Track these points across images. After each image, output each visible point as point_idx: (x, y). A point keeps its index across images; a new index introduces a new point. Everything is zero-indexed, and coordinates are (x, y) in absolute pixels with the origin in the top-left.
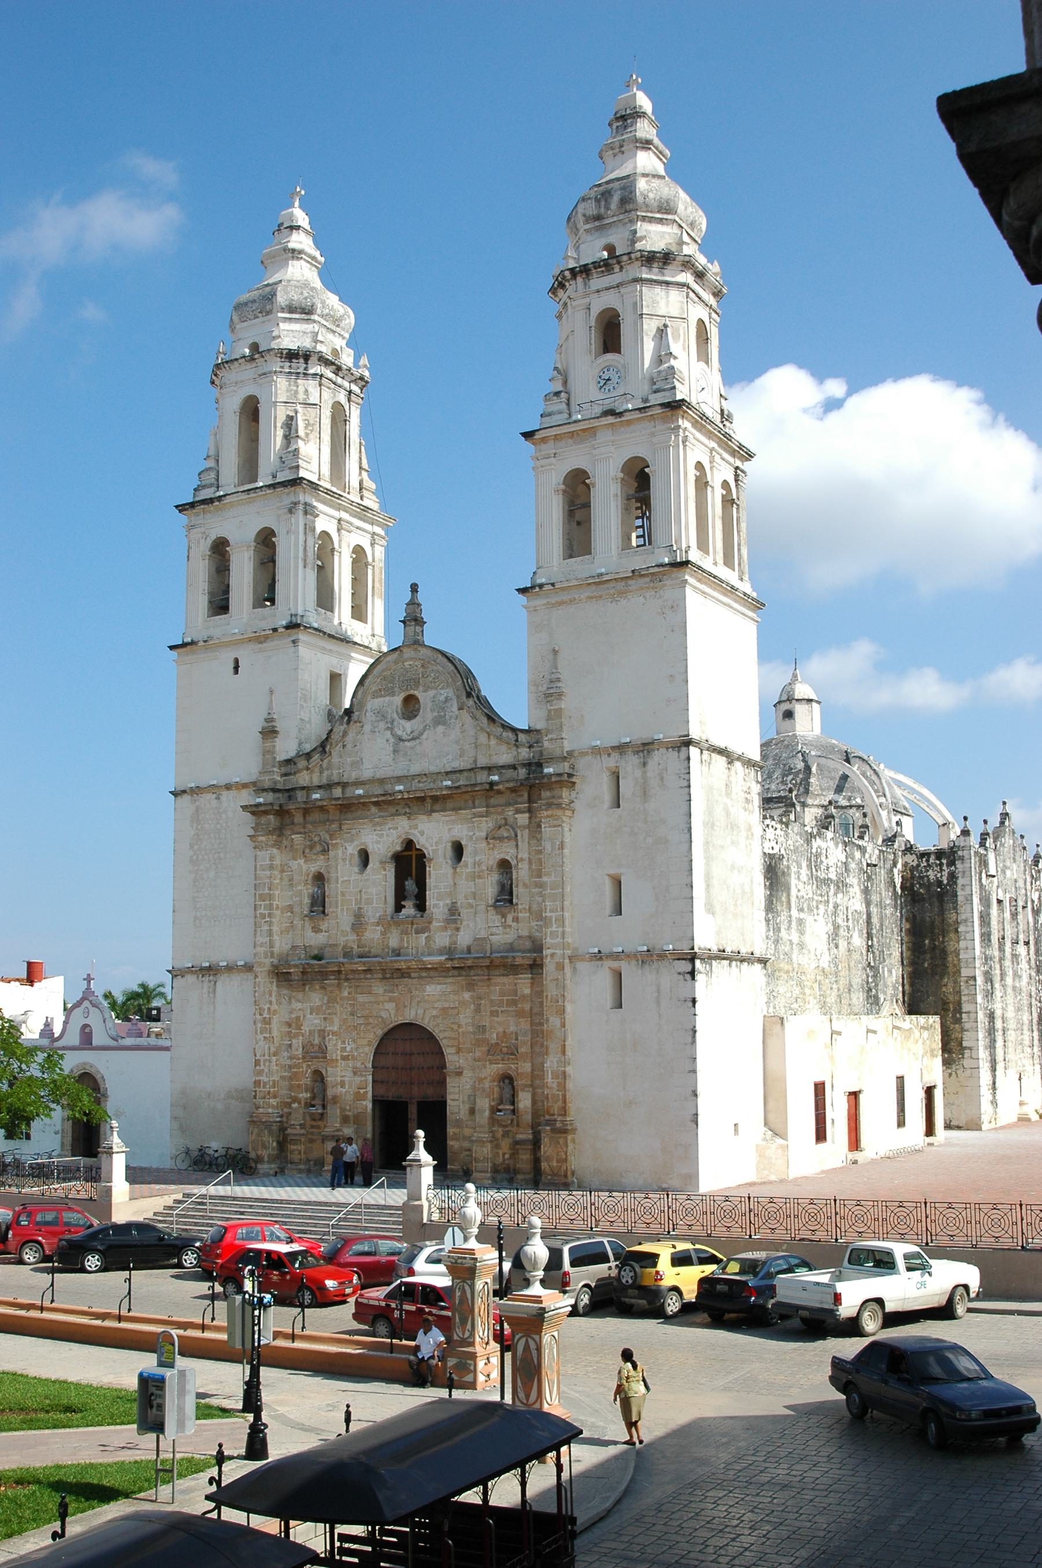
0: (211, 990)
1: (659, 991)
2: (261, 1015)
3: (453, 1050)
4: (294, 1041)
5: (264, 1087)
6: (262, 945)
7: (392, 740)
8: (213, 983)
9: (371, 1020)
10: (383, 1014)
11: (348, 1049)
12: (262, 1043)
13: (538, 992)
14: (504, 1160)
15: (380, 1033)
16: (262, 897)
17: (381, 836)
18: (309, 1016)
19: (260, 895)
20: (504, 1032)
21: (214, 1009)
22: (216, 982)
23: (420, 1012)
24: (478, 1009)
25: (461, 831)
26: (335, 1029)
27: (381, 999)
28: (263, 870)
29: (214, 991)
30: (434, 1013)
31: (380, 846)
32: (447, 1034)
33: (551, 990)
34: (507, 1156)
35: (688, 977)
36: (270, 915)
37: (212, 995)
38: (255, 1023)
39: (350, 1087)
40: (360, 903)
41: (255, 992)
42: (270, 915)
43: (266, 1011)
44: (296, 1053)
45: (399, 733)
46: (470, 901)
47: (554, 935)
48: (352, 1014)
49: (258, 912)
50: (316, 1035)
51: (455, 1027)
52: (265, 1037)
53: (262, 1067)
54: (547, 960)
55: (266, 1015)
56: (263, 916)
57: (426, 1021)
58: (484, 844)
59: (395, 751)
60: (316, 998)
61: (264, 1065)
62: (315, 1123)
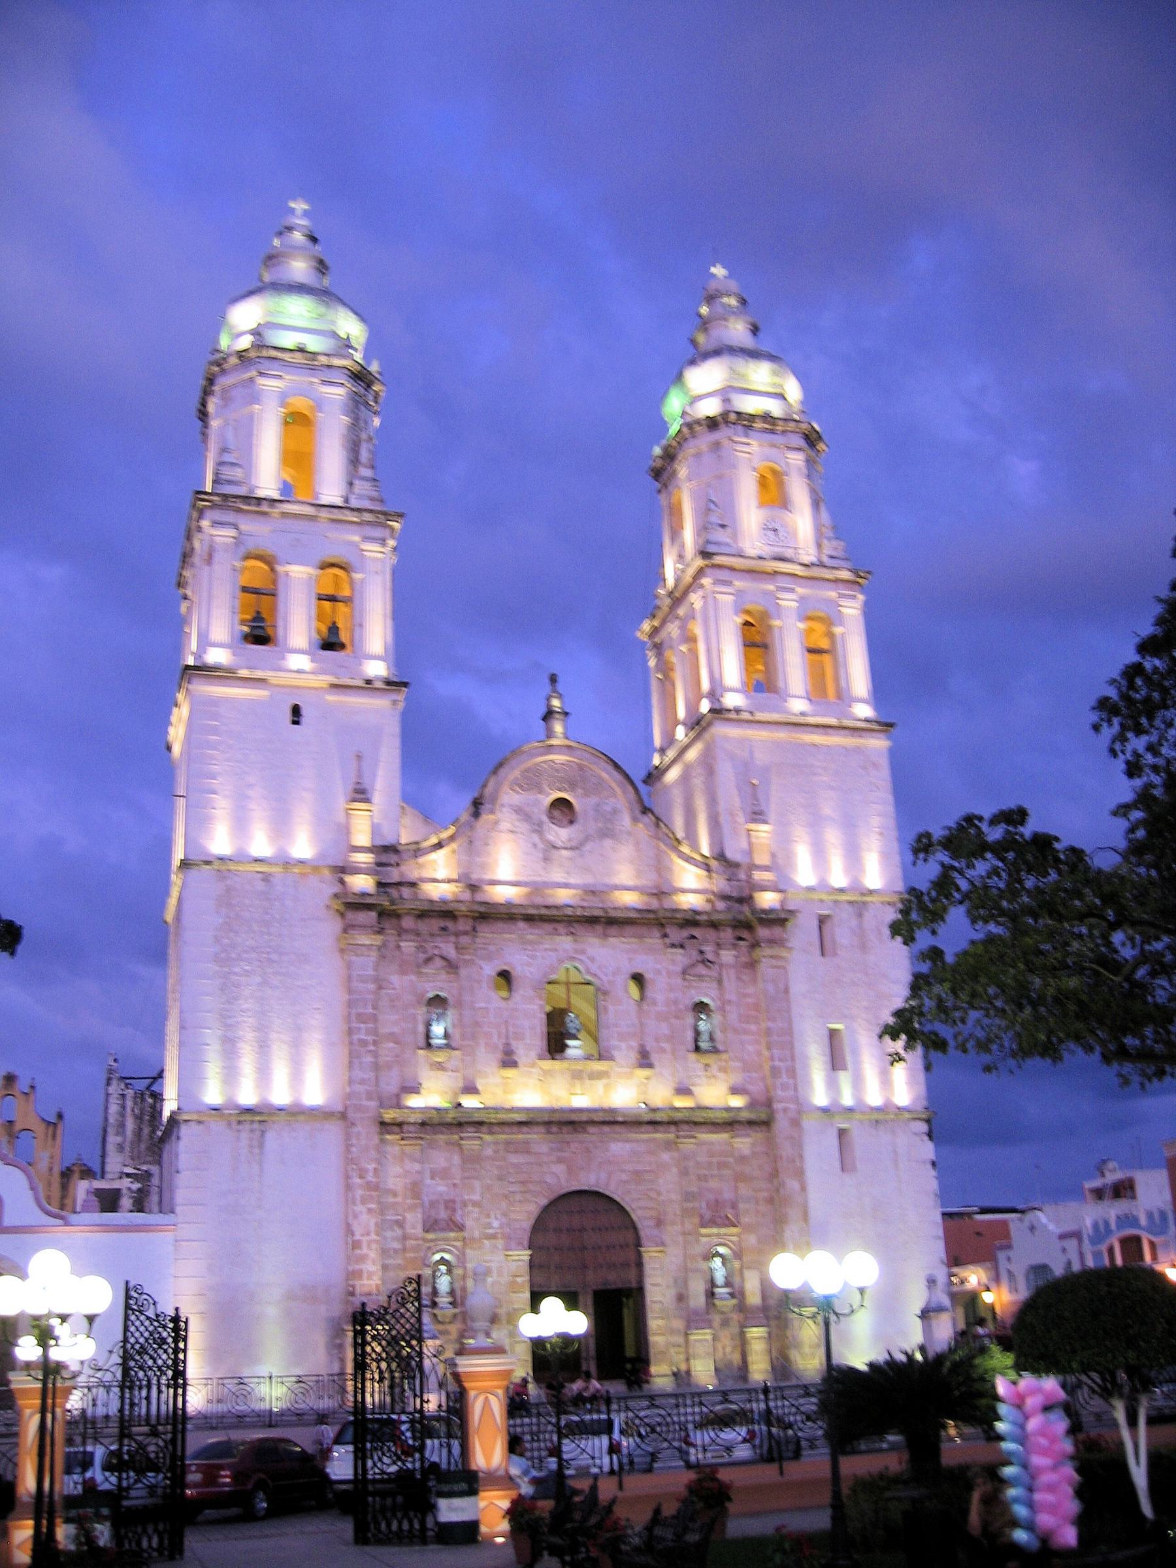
0: (255, 1143)
1: (895, 1152)
2: (361, 1177)
3: (651, 1223)
4: (409, 1216)
5: (369, 1278)
6: (362, 1082)
7: (541, 846)
8: (258, 1133)
9: (531, 1187)
10: (549, 1179)
11: (496, 1224)
12: (365, 1217)
13: (771, 1151)
14: (724, 1354)
15: (544, 1202)
16: (361, 1018)
17: (533, 957)
18: (428, 1181)
19: (359, 1015)
20: (717, 1201)
21: (261, 1170)
22: (263, 1132)
23: (603, 1176)
24: (684, 1172)
25: (645, 963)
26: (476, 1197)
27: (545, 1159)
28: (363, 982)
29: (261, 1146)
30: (624, 1177)
31: (532, 970)
32: (642, 1204)
33: (786, 1150)
34: (728, 1350)
35: (926, 1138)
36: (375, 1043)
37: (257, 1151)
38: (348, 1187)
39: (500, 1274)
40: (507, 1037)
41: (352, 1145)
42: (375, 1043)
43: (371, 1174)
44: (413, 1231)
45: (551, 838)
46: (663, 1045)
47: (784, 1087)
48: (500, 1178)
49: (356, 1037)
50: (442, 1207)
51: (653, 1195)
52: (370, 1210)
53: (365, 1250)
54: (779, 1116)
55: (370, 1177)
56: (363, 1043)
57: (612, 1187)
58: (679, 981)
59: (546, 859)
60: (441, 1158)
61: (369, 1246)
62: (441, 1327)
